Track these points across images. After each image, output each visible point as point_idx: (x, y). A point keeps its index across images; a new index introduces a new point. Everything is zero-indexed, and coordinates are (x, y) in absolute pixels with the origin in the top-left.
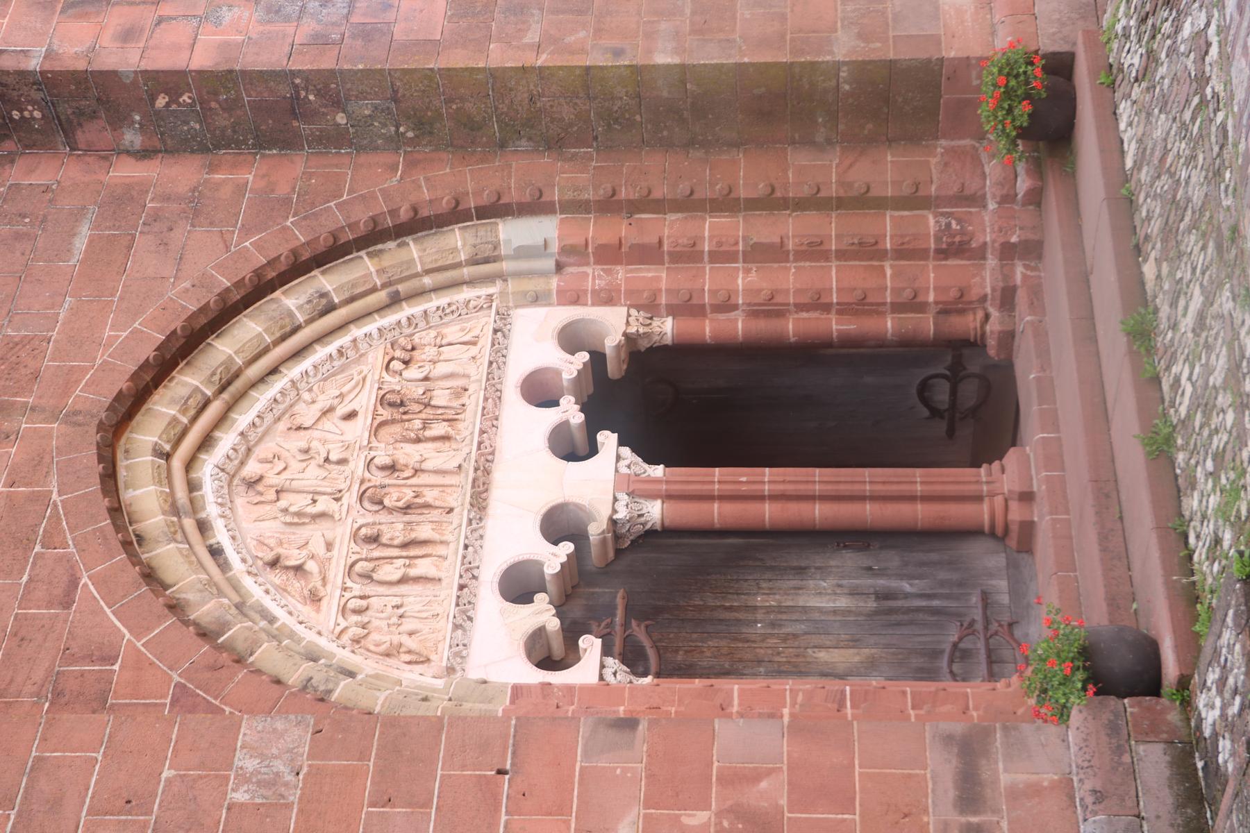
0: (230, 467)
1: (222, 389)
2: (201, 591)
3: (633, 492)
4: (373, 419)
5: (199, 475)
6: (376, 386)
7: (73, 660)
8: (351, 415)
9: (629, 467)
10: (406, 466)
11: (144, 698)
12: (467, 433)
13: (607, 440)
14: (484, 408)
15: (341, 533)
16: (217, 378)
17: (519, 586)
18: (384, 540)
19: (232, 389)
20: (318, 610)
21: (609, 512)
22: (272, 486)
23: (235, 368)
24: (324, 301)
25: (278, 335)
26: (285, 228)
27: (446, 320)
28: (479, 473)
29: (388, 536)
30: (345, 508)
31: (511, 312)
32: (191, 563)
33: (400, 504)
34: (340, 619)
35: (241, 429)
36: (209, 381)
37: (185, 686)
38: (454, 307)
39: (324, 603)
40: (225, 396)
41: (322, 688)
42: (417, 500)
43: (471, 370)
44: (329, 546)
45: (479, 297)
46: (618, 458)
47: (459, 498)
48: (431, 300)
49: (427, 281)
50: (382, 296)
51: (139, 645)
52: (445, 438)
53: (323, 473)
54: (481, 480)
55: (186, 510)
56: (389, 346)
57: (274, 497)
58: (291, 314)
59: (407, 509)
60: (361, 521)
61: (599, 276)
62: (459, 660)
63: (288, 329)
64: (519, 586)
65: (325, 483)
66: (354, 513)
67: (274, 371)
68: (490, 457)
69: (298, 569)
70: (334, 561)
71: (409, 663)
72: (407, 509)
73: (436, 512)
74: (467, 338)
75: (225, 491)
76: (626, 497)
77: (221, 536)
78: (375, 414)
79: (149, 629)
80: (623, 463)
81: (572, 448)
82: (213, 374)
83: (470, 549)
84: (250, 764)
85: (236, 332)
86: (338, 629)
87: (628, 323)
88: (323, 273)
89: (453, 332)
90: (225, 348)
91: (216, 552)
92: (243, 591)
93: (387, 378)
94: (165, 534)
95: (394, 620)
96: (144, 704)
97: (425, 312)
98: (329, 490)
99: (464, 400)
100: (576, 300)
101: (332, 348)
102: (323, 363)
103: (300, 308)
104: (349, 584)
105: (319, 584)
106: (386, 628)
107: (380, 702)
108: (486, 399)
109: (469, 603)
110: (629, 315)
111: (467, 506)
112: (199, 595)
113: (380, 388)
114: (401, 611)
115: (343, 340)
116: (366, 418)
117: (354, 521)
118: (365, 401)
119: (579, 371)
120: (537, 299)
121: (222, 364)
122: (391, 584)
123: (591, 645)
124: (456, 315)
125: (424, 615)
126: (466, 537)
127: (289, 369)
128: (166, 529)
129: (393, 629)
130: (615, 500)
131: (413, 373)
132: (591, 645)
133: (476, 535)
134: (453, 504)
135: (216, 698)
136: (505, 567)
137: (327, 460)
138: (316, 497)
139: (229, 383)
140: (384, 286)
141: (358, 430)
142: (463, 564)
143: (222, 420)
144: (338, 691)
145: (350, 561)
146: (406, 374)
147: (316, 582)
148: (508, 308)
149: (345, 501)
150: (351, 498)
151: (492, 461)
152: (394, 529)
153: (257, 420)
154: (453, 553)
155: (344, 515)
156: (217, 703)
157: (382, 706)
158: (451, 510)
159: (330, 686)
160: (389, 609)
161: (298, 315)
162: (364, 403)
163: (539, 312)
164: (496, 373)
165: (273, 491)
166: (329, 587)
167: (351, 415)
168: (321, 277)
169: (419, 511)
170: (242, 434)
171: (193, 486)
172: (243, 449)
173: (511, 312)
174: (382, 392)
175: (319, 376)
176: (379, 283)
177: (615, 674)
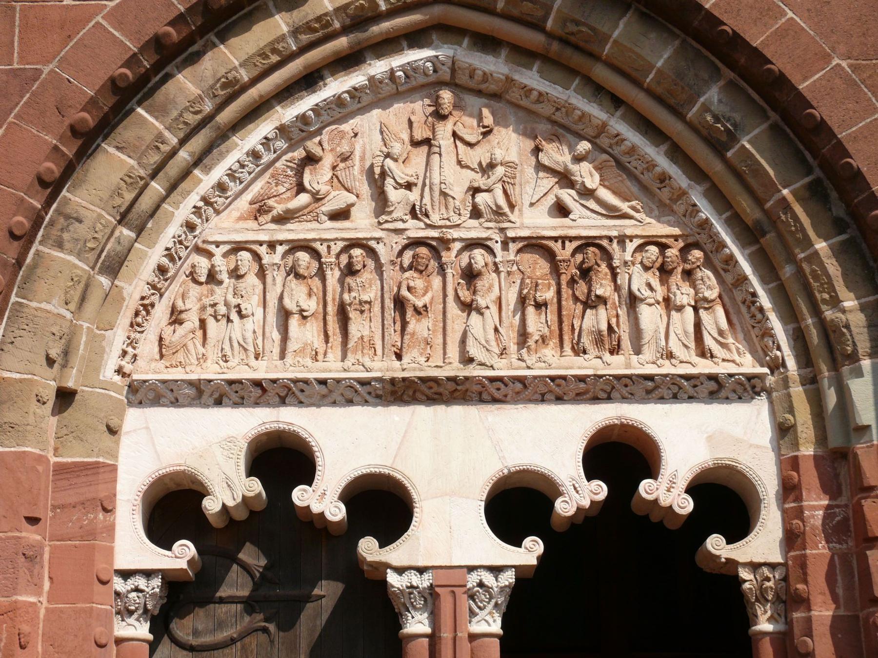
0: (463, 79)
1: (564, 41)
2: (214, 76)
3: (438, 595)
4: (555, 239)
5: (436, 42)
6: (615, 233)
8: (561, 210)
9: (481, 584)
10: (475, 293)
11: (21, 39)
12: (529, 363)
13: (530, 552)
14: (564, 378)
16: (572, 28)
17: (282, 461)
18: (349, 280)
19: (568, 52)
20: (241, 218)
21: (396, 563)
22: (434, 133)
23: (594, 48)
24: (724, 138)
25: (659, 90)
26: (827, 58)
27: (744, 309)
28: (451, 386)
29: (353, 285)
30: (400, 225)
31: (764, 396)
32: (263, 55)
33: (404, 292)
34: (225, 248)
35: (516, 77)
36: (564, 20)
37: (35, 80)
38: (759, 316)
39: (252, 224)
40: (555, 46)
41: (66, 236)
42: (410, 313)
43: (648, 353)
44: (341, 215)
45: (779, 348)
46: (496, 570)
47: (415, 365)
48: (764, 281)
49: (787, 271)
51: (99, 19)
52: (523, 336)
53: (458, 191)
54: (441, 390)
56: (690, 240)
57: (419, 135)
58: (692, 101)
59: (400, 304)
60: (380, 248)
61: (834, 515)
62: (151, 395)
63: (672, 102)
64: (282, 461)
65: (437, 194)
66: (396, 238)
67: (616, 102)
68: (485, 396)
69: (301, 188)
70: (315, 225)
71: (161, 339)
72: (400, 304)
73: (397, 338)
74: (709, 342)
75: (422, 80)
76: (426, 584)
77: (336, 86)
78: (564, 239)
79: (120, 25)
80: (488, 579)
81: (516, 505)
82: (577, 23)
83: (323, 389)
85: (653, 35)
86: (212, 248)
87: (755, 567)
88: (774, 128)
89: (715, 319)
91: (309, 81)
92: (251, 126)
93: (631, 246)
94: (305, 17)
95: (222, 309)
96: (13, 42)
97: (746, 278)
98: (427, 200)
99: (593, 351)
100: (789, 490)
101: (664, 163)
102: (642, 158)
103: (706, 108)
104: (280, 249)
105: (274, 213)
106: (207, 301)
107: (43, 305)
108: (582, 379)
109: (243, 398)
110: (773, 566)
111: (388, 375)
112: (208, 73)
113: (610, 239)
114: (234, 316)
115: (680, 178)
116: (554, 228)
117: (378, 240)
118: (585, 222)
119: (656, 501)
120: (784, 431)
121: (593, 29)
122: (281, 298)
123: (182, 555)
124: (752, 322)
125: (227, 347)
126: (338, 381)
127: (623, 118)
128: (311, 17)
129: (210, 311)
130: (421, 570)
131: (639, 280)
132: (182, 555)
133: (349, 394)
134: (406, 359)
135: (16, 117)
136: (304, 435)
137: (476, 190)
138: (416, 191)
139: (577, 48)
140: (766, 212)
142: (296, 381)
143: (524, 55)
144: (61, 255)
145: (317, 245)
146: (637, 269)
147: (279, 208)
148: (769, 392)
149: (411, 223)
150: (415, 229)
151: (482, 401)
153: (535, 93)
154: (332, 367)
155: (386, 226)
156: (11, 119)
157: (36, 309)
158: (399, 357)
159: (67, 245)
160: (234, 301)
161: (695, 109)
162: (580, 222)
164: (639, 390)
165: (428, 134)
166: (273, 226)
168: (764, 126)
169: (398, 318)
170: (509, 80)
171: (415, 38)
172: (493, 87)
173: (764, 396)
174: (605, 243)
175: (624, 159)
176: (768, 205)
177: (137, 590)
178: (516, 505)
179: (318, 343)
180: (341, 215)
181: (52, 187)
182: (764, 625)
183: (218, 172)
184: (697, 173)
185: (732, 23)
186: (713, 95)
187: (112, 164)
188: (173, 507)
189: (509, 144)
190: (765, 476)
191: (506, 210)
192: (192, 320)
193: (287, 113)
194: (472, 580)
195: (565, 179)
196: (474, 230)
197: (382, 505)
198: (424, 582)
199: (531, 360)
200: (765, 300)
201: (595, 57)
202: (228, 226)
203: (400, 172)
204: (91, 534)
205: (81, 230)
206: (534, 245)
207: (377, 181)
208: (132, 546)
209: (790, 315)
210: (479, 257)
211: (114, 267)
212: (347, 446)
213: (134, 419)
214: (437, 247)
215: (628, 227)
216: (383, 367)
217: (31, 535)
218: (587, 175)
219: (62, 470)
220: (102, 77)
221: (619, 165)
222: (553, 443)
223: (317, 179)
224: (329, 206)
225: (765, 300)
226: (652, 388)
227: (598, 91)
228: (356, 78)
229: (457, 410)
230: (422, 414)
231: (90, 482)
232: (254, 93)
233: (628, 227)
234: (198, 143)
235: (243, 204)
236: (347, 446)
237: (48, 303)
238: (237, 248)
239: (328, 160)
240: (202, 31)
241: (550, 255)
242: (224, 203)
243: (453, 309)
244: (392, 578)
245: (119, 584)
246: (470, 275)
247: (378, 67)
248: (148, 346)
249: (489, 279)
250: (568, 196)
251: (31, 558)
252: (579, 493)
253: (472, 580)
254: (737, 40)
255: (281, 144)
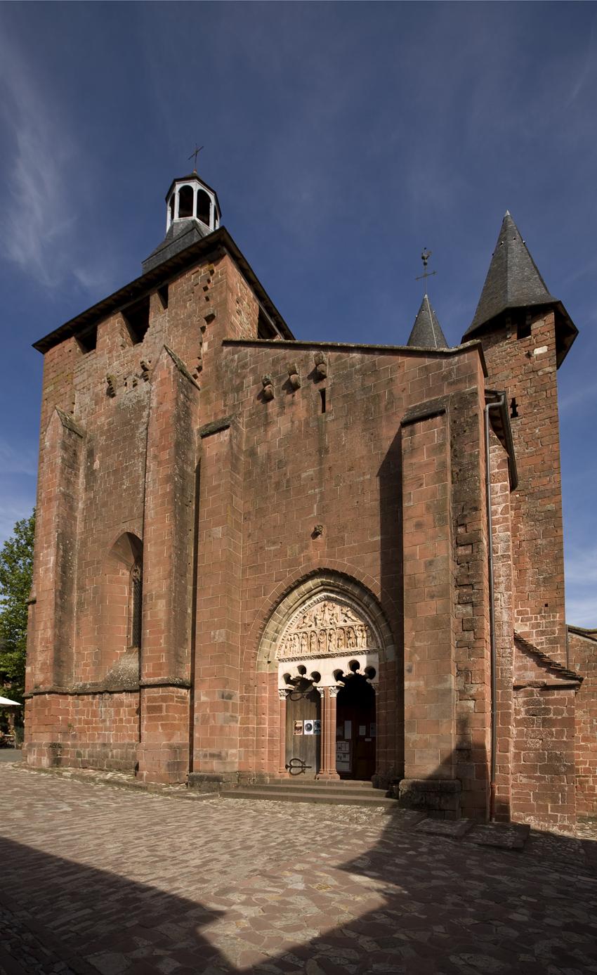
7: (264, 587)
15: (313, 628)
17: (303, 670)
44: (310, 626)
47: (322, 652)
50: (374, 619)
53: (328, 620)
55: (310, 594)
64: (303, 670)
72: (319, 641)
77: (308, 603)
80: (332, 688)
81: (338, 675)
84: (217, 633)
90: (350, 587)
91: (304, 602)
100: (380, 670)
101: (361, 611)
115: (364, 614)
118: (349, 623)
137: (331, 619)
141: (342, 624)
147: (300, 626)
152: (314, 639)
154: (309, 654)
163: (378, 661)
167: (346, 621)
171: (320, 592)
178: (338, 675)
179: (307, 650)
180: (310, 626)
181: (263, 629)
182: (377, 694)
183: (291, 621)
184: (367, 613)
185: (366, 585)
186: (366, 598)
187: (273, 624)
188: (287, 678)
189: (338, 608)
190: (376, 667)
191: (336, 622)
192: (288, 647)
193: (300, 609)
194: (330, 688)
195: (346, 615)
196: (331, 627)
197: (317, 676)
198: (322, 689)
199: (339, 650)
200: (377, 635)
201: (348, 592)
202: (293, 630)
203: (318, 617)
204: (274, 684)
205: (268, 635)
206: (341, 628)
207: (315, 619)
208: (282, 684)
209: (380, 639)
210: (332, 631)
211: (275, 640)
212: (311, 666)
213: (281, 664)
214: (325, 630)
215: (356, 623)
216: (316, 653)
217: (263, 685)
218: (350, 614)
219: (269, 674)
220: (268, 609)
221: (355, 611)
222: (343, 665)
223: (307, 620)
224: (309, 625)
225: (377, 635)
226: (358, 653)
227: (350, 598)
228: (312, 601)
229: (328, 659)
230: (323, 660)
231: (273, 676)
232: (294, 607)
233: (356, 623)
234: (286, 617)
235: (296, 626)
236: (311, 666)
237: (265, 648)
238: (295, 634)
239: (308, 617)
240: (284, 598)
241: (343, 630)
242: (293, 625)
243: (328, 641)
244: (318, 689)
245: (279, 692)
246: (330, 635)
247: (315, 598)
248: (282, 652)
249: (333, 635)
250: (346, 618)
251: (265, 688)
252: (347, 671)
253: (330, 688)
254: (367, 588)
255: (301, 614)
